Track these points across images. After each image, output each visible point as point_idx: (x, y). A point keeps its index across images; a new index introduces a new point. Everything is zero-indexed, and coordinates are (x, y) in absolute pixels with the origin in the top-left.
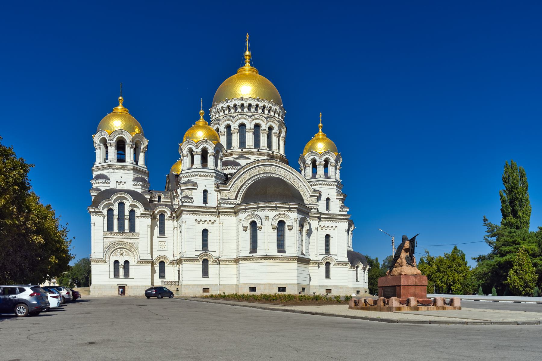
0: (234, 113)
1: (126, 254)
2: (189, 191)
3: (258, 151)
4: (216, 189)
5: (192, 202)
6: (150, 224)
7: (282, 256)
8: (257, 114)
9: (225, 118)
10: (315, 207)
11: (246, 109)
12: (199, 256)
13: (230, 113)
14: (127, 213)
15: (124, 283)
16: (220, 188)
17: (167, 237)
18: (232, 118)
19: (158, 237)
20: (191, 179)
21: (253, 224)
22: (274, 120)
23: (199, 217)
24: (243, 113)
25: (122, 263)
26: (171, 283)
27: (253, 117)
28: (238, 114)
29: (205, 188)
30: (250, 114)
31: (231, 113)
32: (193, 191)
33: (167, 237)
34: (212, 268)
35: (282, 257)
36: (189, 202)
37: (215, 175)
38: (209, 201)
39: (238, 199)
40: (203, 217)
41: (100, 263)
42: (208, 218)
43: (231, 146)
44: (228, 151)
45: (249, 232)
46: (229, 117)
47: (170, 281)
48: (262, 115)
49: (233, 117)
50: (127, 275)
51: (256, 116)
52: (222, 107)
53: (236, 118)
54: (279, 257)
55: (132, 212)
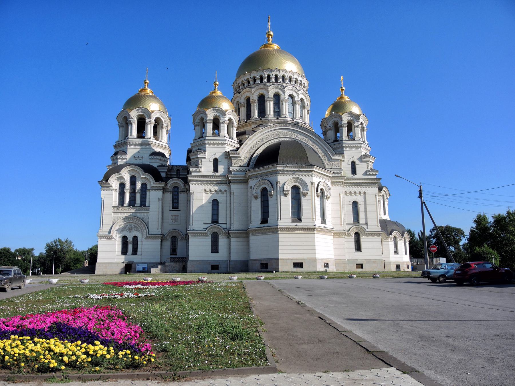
1: (135, 229)
3: (278, 119)
4: (226, 157)
5: (201, 172)
6: (161, 197)
7: (296, 225)
10: (338, 171)
11: (266, 80)
12: (207, 229)
14: (139, 185)
15: (132, 260)
16: (231, 155)
17: (180, 211)
19: (170, 211)
21: (264, 190)
22: (294, 88)
25: (130, 239)
26: (181, 260)
27: (271, 87)
30: (268, 84)
31: (250, 85)
32: (203, 160)
33: (180, 211)
34: (222, 242)
35: (297, 227)
36: (197, 172)
39: (250, 166)
41: (107, 240)
43: (250, 117)
44: (247, 121)
45: (259, 200)
47: (176, 258)
48: (281, 84)
50: (135, 252)
51: (275, 86)
54: (293, 227)
55: (144, 185)
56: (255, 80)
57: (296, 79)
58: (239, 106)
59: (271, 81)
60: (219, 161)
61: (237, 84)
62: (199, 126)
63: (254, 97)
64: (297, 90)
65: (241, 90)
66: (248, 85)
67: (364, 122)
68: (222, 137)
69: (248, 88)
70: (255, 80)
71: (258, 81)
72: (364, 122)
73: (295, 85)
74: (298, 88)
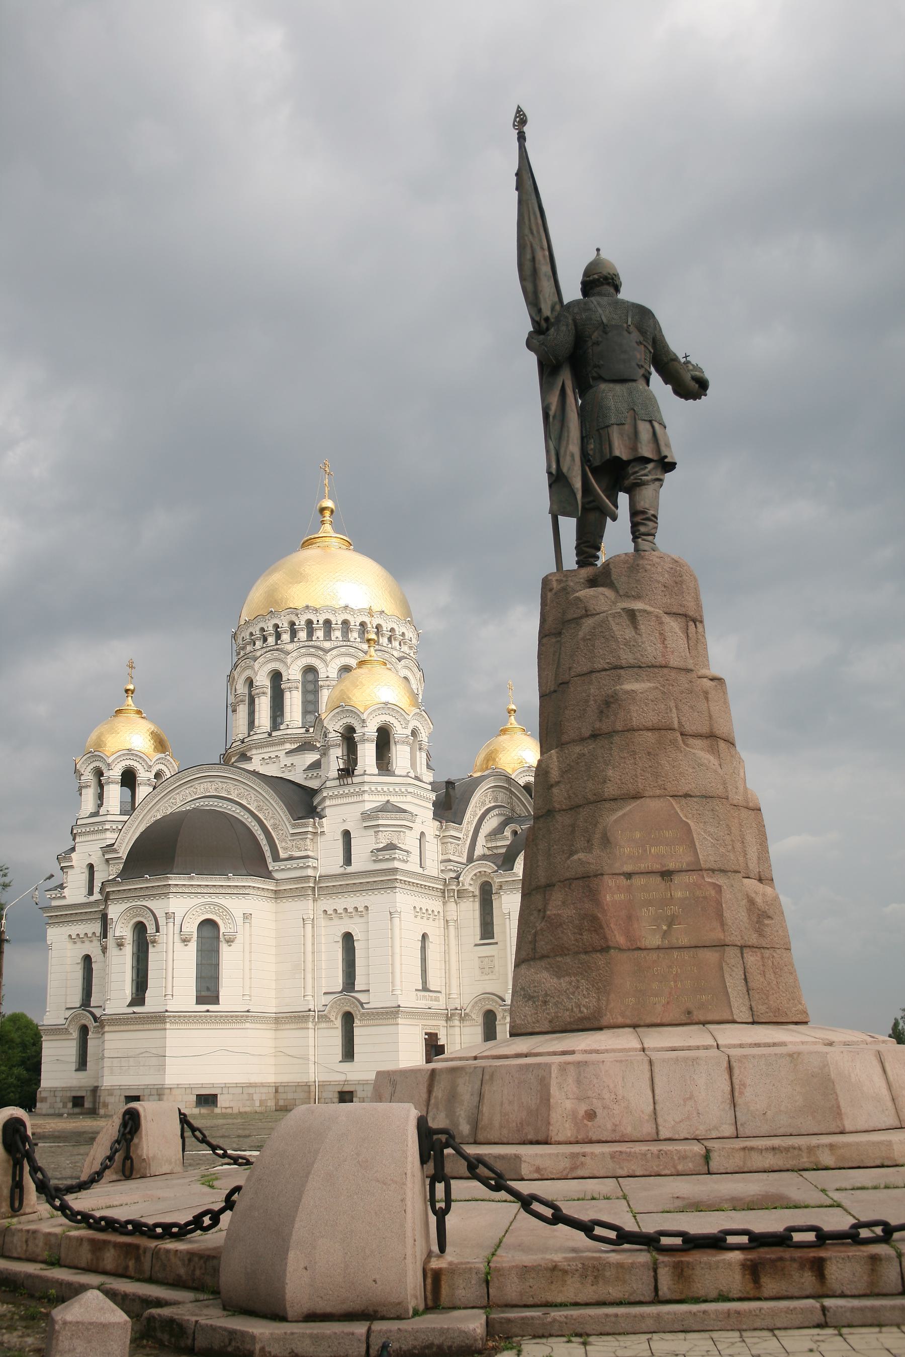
8: (345, 643)
9: (268, 655)
11: (320, 634)
24: (310, 643)
27: (334, 652)
28: (302, 644)
30: (327, 645)
46: (276, 653)
51: (343, 650)
53: (294, 654)
56: (294, 633)
57: (392, 630)
59: (333, 638)
63: (293, 673)
64: (394, 660)
65: (258, 654)
66: (277, 644)
69: (277, 650)
70: (294, 633)
71: (302, 635)
73: (390, 646)
74: (396, 654)
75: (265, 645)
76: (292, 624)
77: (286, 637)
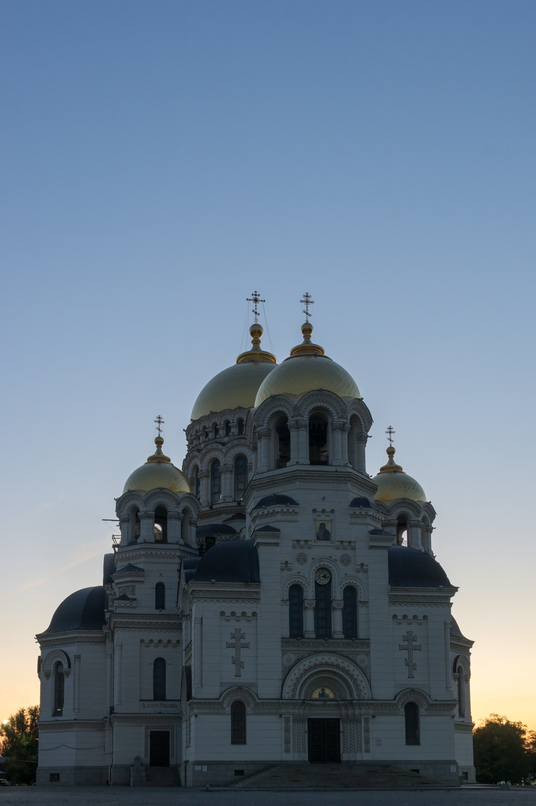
0: (224, 437)
2: (130, 585)
5: (135, 607)
9: (209, 447)
13: (218, 436)
18: (220, 446)
20: (132, 562)
23: (147, 635)
29: (160, 580)
32: (137, 585)
36: (129, 607)
37: (178, 553)
38: (167, 604)
40: (156, 635)
42: (165, 636)
46: (215, 445)
49: (224, 444)
52: (205, 427)
58: (197, 476)
60: (166, 587)
61: (194, 431)
62: (128, 521)
65: (203, 446)
66: (216, 438)
67: (428, 516)
68: (172, 544)
70: (228, 428)
72: (428, 516)
75: (207, 440)
76: (227, 422)
77: (222, 432)
